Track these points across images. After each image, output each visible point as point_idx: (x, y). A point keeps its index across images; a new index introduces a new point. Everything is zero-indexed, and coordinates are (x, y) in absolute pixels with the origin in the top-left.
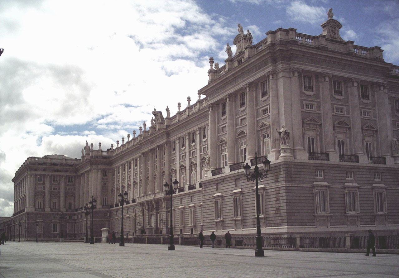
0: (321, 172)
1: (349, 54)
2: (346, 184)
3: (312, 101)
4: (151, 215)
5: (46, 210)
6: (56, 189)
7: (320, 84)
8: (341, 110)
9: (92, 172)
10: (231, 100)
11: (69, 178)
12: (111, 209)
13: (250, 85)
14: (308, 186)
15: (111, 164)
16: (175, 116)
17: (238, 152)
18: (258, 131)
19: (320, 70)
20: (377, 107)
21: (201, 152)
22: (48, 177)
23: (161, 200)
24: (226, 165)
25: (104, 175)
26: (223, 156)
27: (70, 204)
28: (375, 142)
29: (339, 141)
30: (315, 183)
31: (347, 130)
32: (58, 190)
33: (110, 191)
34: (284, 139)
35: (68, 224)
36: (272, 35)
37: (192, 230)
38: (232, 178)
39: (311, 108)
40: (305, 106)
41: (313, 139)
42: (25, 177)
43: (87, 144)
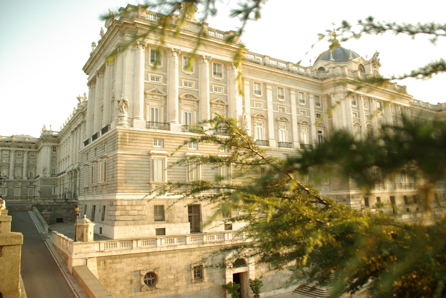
0: (161, 142)
7: (168, 59)
8: (190, 85)
14: (144, 154)
15: (59, 142)
20: (228, 84)
22: (13, 152)
25: (54, 151)
29: (186, 113)
30: (152, 152)
31: (195, 102)
33: (58, 163)
34: (122, 107)
35: (28, 189)
39: (156, 80)
40: (150, 78)
41: (157, 109)
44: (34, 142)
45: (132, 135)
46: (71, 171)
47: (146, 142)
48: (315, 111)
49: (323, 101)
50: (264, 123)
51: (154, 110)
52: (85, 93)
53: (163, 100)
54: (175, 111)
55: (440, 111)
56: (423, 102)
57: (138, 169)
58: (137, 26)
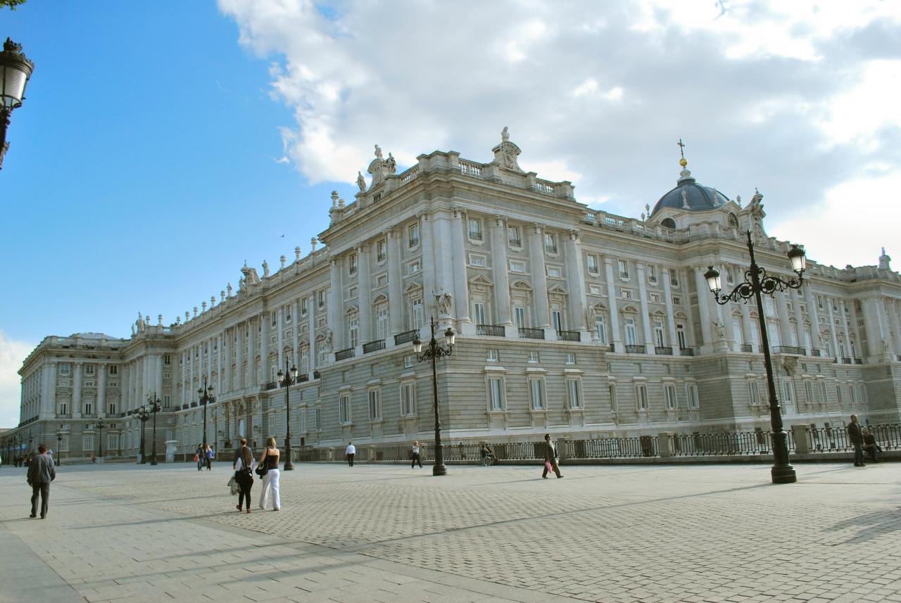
1: (530, 189)
2: (529, 369)
3: (481, 253)
4: (239, 420)
5: (74, 415)
6: (91, 384)
7: (491, 230)
9: (148, 359)
10: (364, 251)
11: (112, 367)
12: (176, 412)
13: (393, 230)
14: (478, 372)
15: (176, 346)
16: (277, 275)
17: (374, 326)
18: (405, 295)
19: (491, 211)
20: (566, 262)
21: (316, 326)
22: (79, 366)
23: (254, 397)
24: (356, 345)
25: (166, 363)
26: (352, 331)
27: (112, 407)
28: (565, 311)
29: (517, 309)
30: (487, 368)
31: (528, 293)
32: (93, 385)
34: (444, 305)
35: (108, 436)
36: (426, 160)
37: (302, 440)
38: (367, 363)
42: (40, 367)
43: (140, 317)
44: (116, 347)
45: (460, 345)
46: (234, 401)
47: (478, 355)
48: (672, 295)
49: (681, 278)
50: (604, 318)
51: (479, 307)
52: (266, 264)
53: (489, 291)
54: (507, 308)
55: (853, 281)
56: (826, 268)
57: (473, 394)
58: (454, 185)
